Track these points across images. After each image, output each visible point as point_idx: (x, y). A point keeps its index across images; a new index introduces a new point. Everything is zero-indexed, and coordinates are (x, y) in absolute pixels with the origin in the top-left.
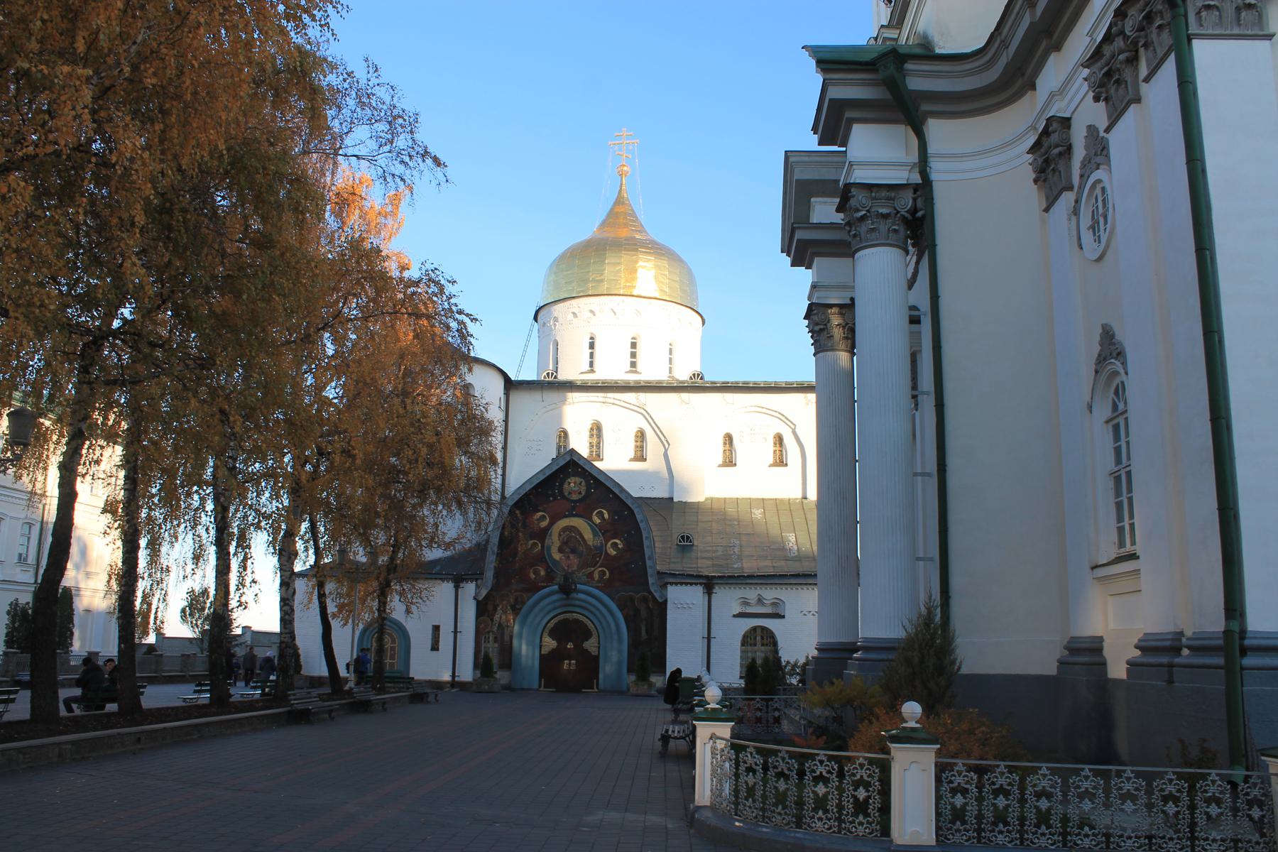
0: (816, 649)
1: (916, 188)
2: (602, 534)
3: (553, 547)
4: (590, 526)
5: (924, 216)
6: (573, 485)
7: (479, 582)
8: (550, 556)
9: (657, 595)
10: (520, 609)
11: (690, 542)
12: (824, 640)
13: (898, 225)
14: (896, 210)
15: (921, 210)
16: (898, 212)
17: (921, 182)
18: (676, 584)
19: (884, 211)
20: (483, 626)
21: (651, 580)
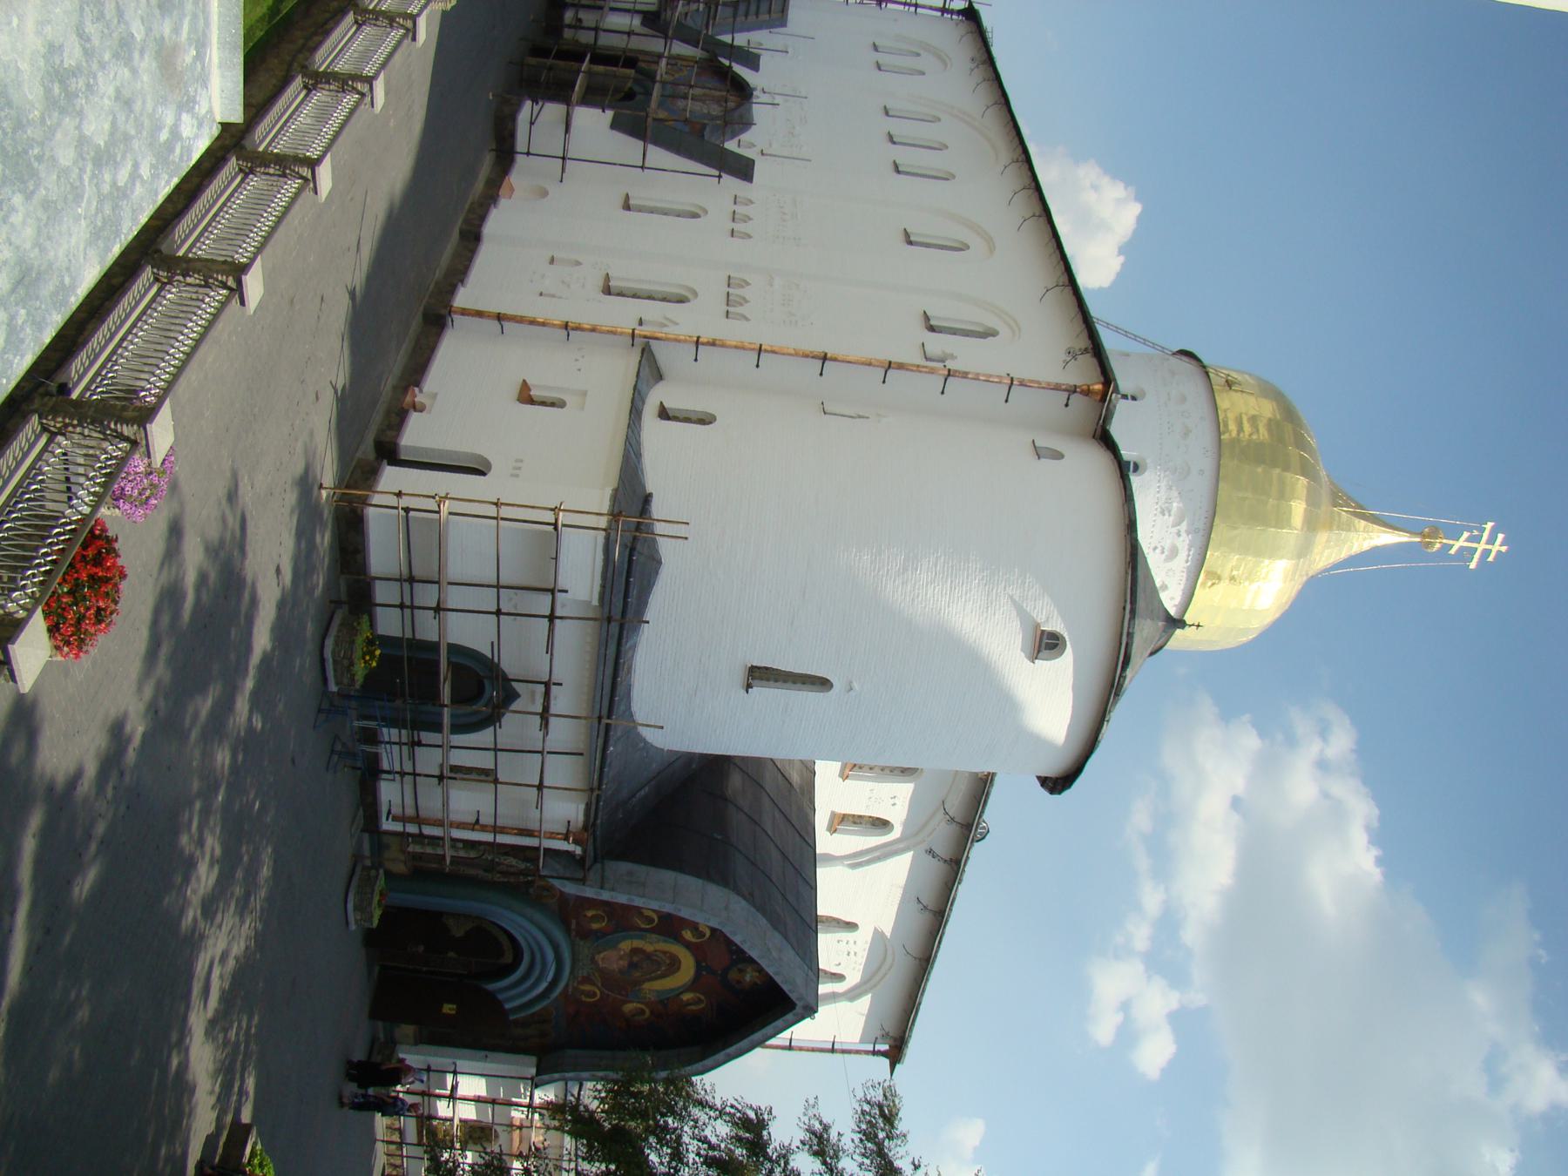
3: (643, 942)
8: (624, 938)
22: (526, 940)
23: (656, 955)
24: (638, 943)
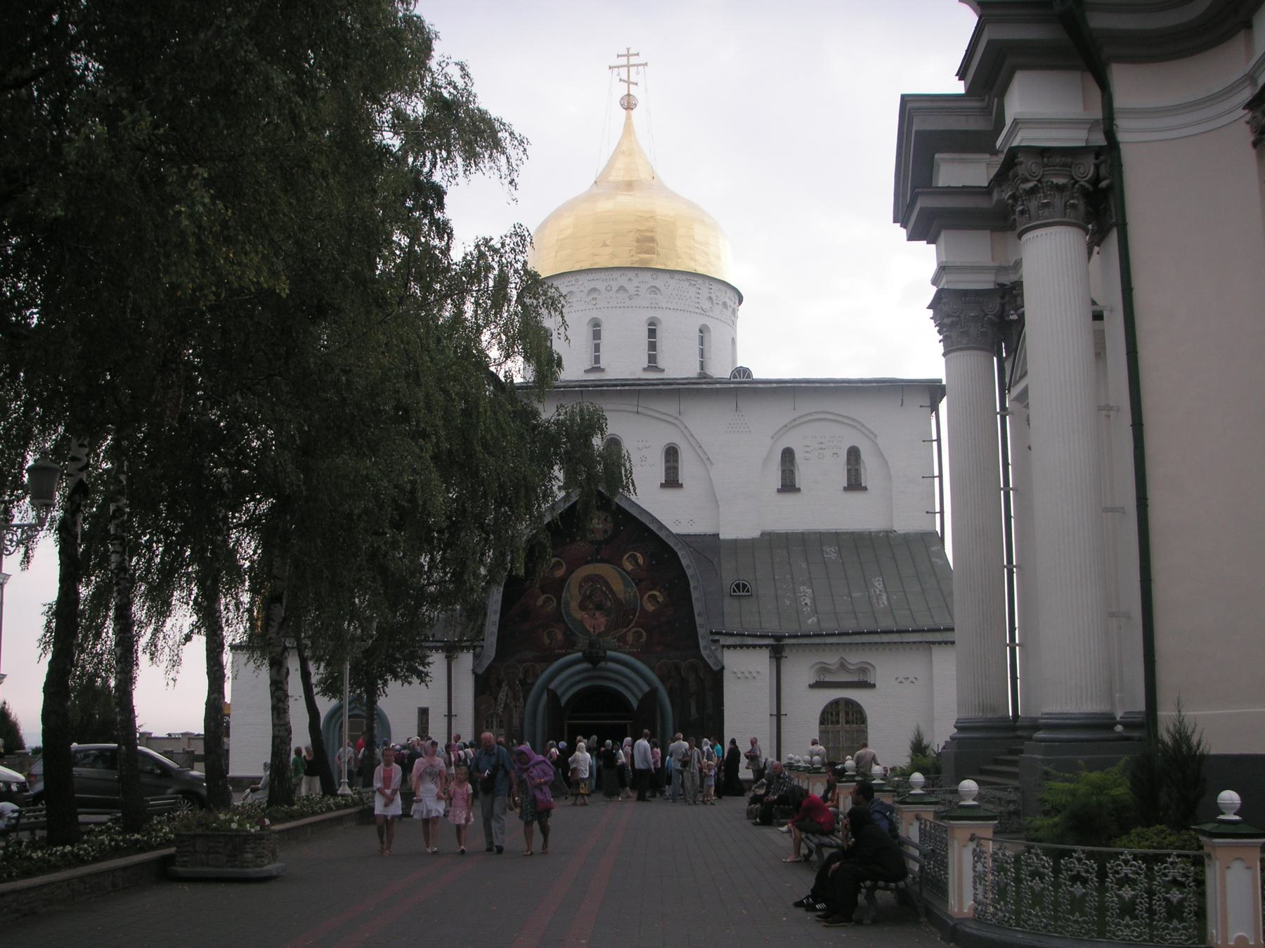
0: (955, 727)
1: (1098, 152)
2: (636, 584)
4: (619, 573)
5: (1110, 187)
6: (598, 524)
7: (478, 650)
9: (710, 662)
10: (533, 684)
11: (748, 591)
12: (964, 715)
13: (1077, 198)
14: (1073, 178)
15: (1105, 179)
16: (1076, 182)
17: (1106, 144)
18: (735, 647)
19: (1061, 181)
20: (483, 707)
21: (702, 643)
22: (579, 682)
23: (585, 592)
24: (574, 605)
